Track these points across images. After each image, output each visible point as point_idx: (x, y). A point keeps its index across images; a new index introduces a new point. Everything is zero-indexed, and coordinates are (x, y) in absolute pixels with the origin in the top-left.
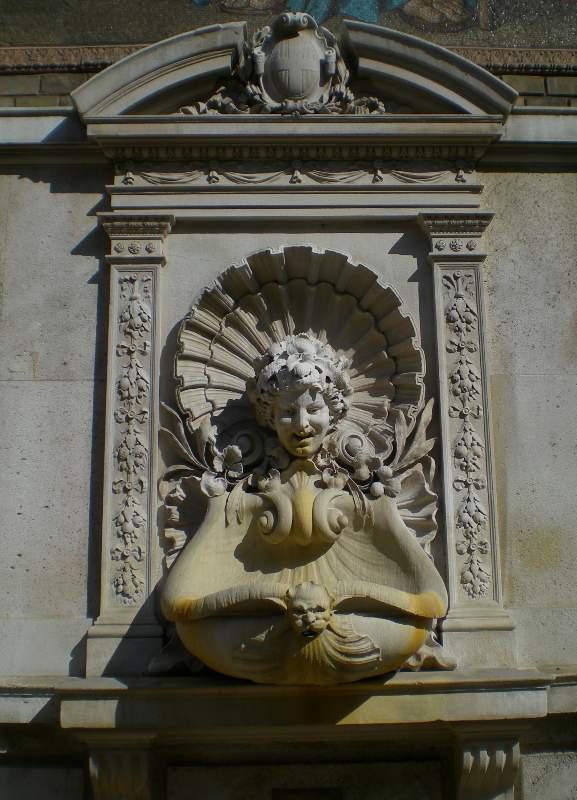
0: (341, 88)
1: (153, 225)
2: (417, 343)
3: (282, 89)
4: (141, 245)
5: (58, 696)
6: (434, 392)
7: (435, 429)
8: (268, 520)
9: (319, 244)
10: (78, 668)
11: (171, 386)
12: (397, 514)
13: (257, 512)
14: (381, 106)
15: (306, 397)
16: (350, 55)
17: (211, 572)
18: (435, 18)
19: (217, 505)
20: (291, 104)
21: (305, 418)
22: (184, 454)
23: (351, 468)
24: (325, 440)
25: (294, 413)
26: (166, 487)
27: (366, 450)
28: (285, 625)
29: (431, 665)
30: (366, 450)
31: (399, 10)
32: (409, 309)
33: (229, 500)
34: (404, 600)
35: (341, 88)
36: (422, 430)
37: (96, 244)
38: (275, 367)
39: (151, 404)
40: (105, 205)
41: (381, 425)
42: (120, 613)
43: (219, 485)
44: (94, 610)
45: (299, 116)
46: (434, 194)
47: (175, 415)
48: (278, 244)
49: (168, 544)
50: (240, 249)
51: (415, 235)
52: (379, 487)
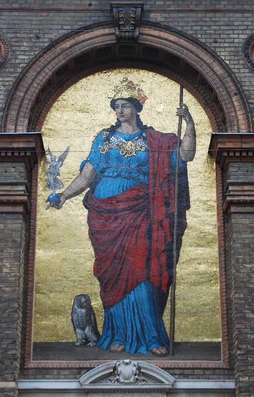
18: (160, 353)
31: (151, 351)
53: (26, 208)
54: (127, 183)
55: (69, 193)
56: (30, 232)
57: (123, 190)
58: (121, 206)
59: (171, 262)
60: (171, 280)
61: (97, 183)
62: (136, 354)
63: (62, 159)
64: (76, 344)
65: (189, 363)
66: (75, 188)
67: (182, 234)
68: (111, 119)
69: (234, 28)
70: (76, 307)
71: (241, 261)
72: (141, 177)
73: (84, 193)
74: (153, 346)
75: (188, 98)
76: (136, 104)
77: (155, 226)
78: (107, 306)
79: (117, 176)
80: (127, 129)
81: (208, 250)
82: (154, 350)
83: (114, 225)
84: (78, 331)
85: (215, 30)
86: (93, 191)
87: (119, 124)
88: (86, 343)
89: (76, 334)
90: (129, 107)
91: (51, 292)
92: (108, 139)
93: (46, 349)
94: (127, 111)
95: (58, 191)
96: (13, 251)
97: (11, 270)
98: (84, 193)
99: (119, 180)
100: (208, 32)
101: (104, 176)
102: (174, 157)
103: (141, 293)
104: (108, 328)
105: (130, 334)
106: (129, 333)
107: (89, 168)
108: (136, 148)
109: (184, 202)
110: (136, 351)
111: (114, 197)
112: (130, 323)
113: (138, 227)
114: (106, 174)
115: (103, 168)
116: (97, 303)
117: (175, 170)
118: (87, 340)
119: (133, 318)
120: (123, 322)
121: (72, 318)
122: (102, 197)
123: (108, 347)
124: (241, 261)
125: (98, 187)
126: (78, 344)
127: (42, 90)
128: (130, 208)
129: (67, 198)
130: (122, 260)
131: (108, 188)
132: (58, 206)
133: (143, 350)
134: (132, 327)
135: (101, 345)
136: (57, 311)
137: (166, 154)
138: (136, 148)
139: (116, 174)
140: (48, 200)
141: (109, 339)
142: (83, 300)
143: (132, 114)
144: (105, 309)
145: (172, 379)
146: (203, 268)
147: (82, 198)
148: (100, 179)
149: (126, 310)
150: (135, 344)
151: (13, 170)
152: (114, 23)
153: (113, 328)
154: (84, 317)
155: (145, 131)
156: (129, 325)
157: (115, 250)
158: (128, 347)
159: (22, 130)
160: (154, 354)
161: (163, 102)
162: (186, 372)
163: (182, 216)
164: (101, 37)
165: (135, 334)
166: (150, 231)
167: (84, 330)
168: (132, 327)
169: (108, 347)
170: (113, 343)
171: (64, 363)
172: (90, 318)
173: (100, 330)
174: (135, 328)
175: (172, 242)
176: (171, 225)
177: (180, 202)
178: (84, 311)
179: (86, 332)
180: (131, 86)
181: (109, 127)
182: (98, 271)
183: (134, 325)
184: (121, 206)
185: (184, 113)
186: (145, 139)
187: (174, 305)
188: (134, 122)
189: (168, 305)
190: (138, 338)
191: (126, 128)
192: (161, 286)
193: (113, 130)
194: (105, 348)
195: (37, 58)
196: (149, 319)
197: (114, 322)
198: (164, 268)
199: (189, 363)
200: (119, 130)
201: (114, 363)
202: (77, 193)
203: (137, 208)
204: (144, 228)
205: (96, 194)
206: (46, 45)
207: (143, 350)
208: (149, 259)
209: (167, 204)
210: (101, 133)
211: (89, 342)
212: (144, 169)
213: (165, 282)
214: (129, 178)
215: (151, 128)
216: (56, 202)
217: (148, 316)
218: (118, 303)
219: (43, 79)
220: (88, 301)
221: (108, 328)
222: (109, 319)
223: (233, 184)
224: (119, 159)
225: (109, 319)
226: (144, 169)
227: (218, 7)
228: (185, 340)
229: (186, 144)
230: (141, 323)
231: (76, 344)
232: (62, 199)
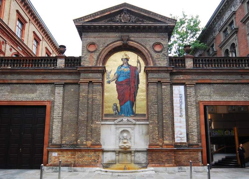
9: (126, 129)
48: (124, 129)
50: (122, 129)
53: (102, 84)
54: (125, 78)
55: (112, 80)
58: (124, 83)
59: (135, 96)
60: (135, 100)
62: (127, 116)
63: (110, 72)
65: (139, 118)
66: (113, 79)
67: (138, 90)
68: (121, 63)
72: (128, 77)
73: (115, 80)
75: (140, 58)
76: (127, 59)
77: (131, 88)
78: (121, 106)
80: (125, 65)
81: (143, 93)
82: (131, 115)
83: (122, 87)
86: (117, 80)
87: (123, 64)
91: (108, 103)
92: (121, 67)
93: (107, 115)
94: (125, 61)
95: (109, 80)
98: (115, 80)
107: (116, 74)
108: (127, 70)
109: (138, 83)
111: (122, 81)
113: (128, 88)
116: (118, 105)
118: (116, 113)
125: (118, 79)
127: (105, 56)
128: (126, 84)
129: (112, 81)
131: (121, 79)
133: (129, 115)
136: (109, 107)
137: (134, 71)
138: (127, 70)
140: (107, 82)
143: (126, 62)
145: (135, 122)
146: (142, 97)
147: (115, 81)
150: (127, 114)
152: (122, 40)
155: (129, 66)
157: (122, 93)
159: (101, 65)
160: (131, 116)
161: (134, 59)
162: (138, 120)
163: (138, 85)
164: (119, 43)
166: (130, 89)
171: (111, 118)
176: (135, 87)
177: (137, 82)
178: (115, 107)
180: (126, 55)
182: (119, 98)
184: (124, 83)
185: (138, 62)
186: (129, 68)
188: (127, 64)
189: (134, 105)
190: (128, 113)
191: (125, 65)
193: (122, 66)
195: (104, 49)
198: (134, 98)
199: (139, 118)
200: (123, 66)
201: (122, 118)
202: (113, 80)
204: (129, 88)
205: (118, 81)
207: (129, 115)
208: (130, 96)
209: (134, 83)
210: (119, 66)
213: (134, 101)
216: (109, 82)
217: (130, 108)
219: (105, 53)
220: (116, 105)
223: (149, 78)
224: (123, 72)
227: (146, 36)
228: (138, 113)
229: (139, 69)
232: (110, 82)
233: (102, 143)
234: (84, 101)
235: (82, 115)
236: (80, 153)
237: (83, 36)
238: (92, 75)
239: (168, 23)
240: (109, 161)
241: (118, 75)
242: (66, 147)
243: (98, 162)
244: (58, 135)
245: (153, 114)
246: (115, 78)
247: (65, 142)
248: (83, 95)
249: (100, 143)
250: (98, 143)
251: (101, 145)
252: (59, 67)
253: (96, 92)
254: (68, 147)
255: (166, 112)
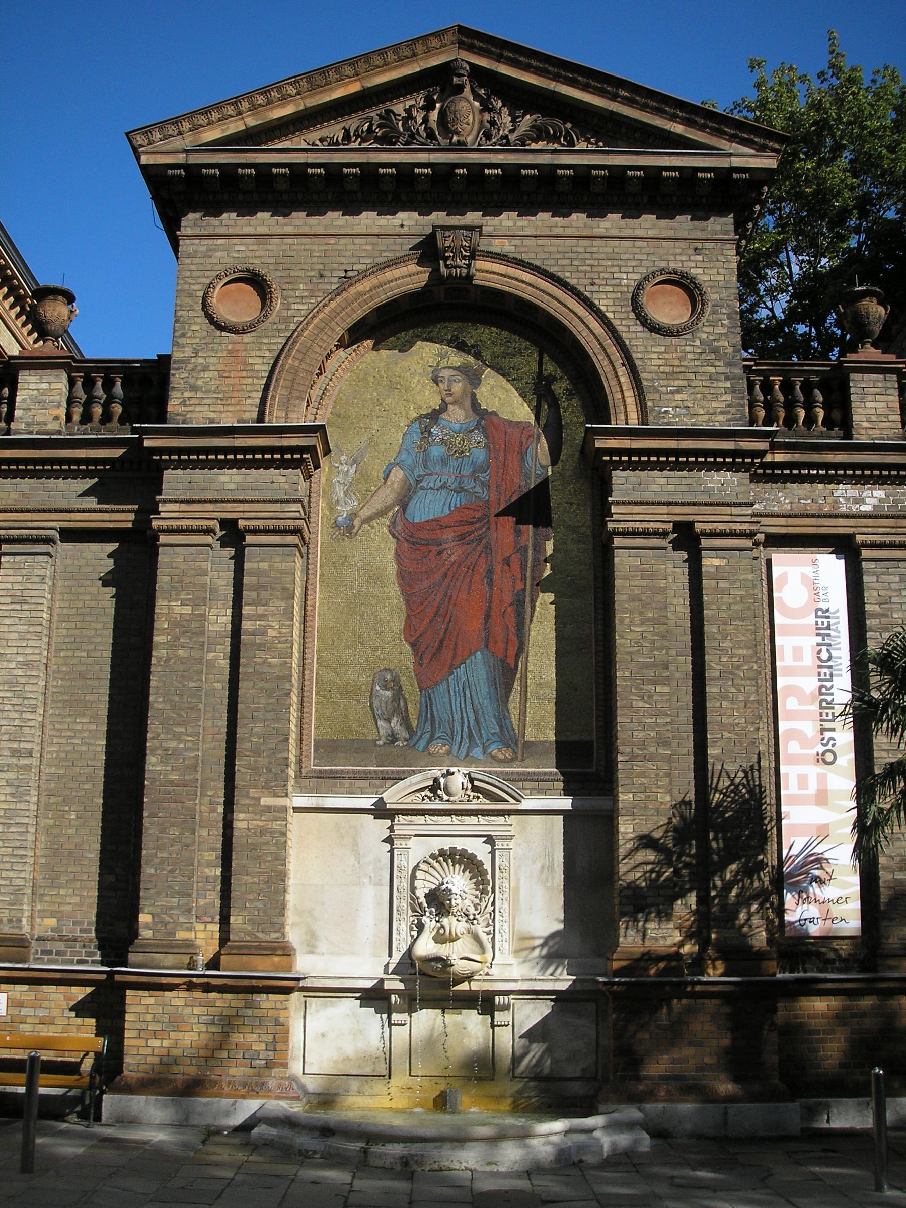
0: (468, 792)
1: (407, 837)
2: (489, 877)
3: (448, 794)
4: (403, 843)
5: (382, 981)
6: (493, 892)
7: (493, 904)
8: (442, 931)
9: (460, 844)
10: (386, 972)
11: (413, 889)
12: (480, 929)
13: (439, 929)
14: (481, 796)
15: (454, 896)
16: (471, 780)
17: (426, 947)
19: (427, 926)
20: (452, 799)
21: (453, 902)
22: (417, 909)
23: (467, 915)
24: (459, 907)
25: (450, 900)
26: (412, 919)
27: (472, 910)
28: (445, 963)
29: (487, 974)
30: (472, 910)
32: (487, 866)
33: (430, 923)
34: (478, 958)
35: (468, 792)
36: (490, 904)
37: (389, 840)
38: (444, 887)
39: (406, 894)
40: (391, 829)
41: (477, 901)
42: (397, 957)
43: (428, 920)
44: (390, 955)
45: (454, 802)
46: (496, 826)
47: (414, 898)
48: (447, 844)
49: (412, 936)
51: (490, 840)
52: (475, 922)
54: (457, 500)
56: (307, 574)
57: (450, 509)
61: (410, 499)
62: (468, 759)
64: (378, 743)
69: (620, 263)
70: (378, 688)
71: (627, 621)
72: (478, 489)
74: (493, 747)
75: (550, 368)
77: (498, 568)
79: (441, 487)
84: (381, 723)
85: (592, 266)
86: (404, 507)
87: (444, 407)
88: (393, 742)
89: (378, 729)
90: (459, 381)
92: (427, 431)
94: (457, 387)
96: (283, 604)
97: (280, 633)
98: (390, 514)
99: (444, 492)
100: (581, 268)
101: (422, 488)
102: (529, 459)
103: (476, 670)
104: (426, 721)
105: (459, 729)
106: (457, 727)
107: (397, 475)
110: (467, 755)
111: (436, 520)
112: (459, 713)
114: (423, 484)
115: (419, 476)
117: (530, 478)
118: (393, 738)
119: (463, 706)
120: (449, 712)
121: (371, 704)
122: (417, 520)
123: (426, 747)
124: (627, 621)
126: (381, 743)
130: (448, 616)
131: (429, 507)
132: (351, 533)
133: (477, 752)
134: (462, 718)
135: (414, 746)
139: (439, 484)
141: (428, 736)
142: (389, 677)
143: (464, 391)
144: (421, 691)
148: (415, 492)
149: (452, 693)
151: (283, 479)
153: (433, 721)
154: (389, 703)
156: (457, 717)
158: (455, 748)
160: (494, 758)
165: (466, 729)
167: (390, 722)
168: (462, 718)
169: (426, 747)
170: (435, 742)
172: (399, 704)
173: (414, 724)
174: (466, 720)
175: (524, 590)
178: (389, 693)
179: (392, 725)
181: (430, 411)
183: (465, 715)
187: (526, 687)
188: (468, 403)
189: (517, 685)
192: (506, 657)
193: (435, 416)
194: (421, 749)
195: (318, 308)
196: (488, 708)
197: (434, 709)
201: (437, 772)
203: (472, 537)
204: (482, 569)
206: (334, 287)
207: (477, 752)
211: (397, 740)
212: (483, 477)
213: (512, 652)
214: (460, 490)
215: (495, 413)
218: (442, 680)
221: (426, 721)
222: (426, 706)
223: (617, 503)
225: (426, 706)
226: (483, 477)
230: (475, 712)
231: (378, 743)
233: (294, 936)
234: (181, 653)
235: (166, 750)
236: (151, 1000)
237: (189, 231)
238: (239, 478)
239: (731, 155)
240: (347, 1059)
241: (405, 480)
242: (58, 953)
243: (269, 1065)
244: (11, 874)
245: (643, 745)
246: (389, 501)
247: (52, 922)
248: (178, 610)
249: (283, 935)
250: (274, 936)
251: (286, 951)
252: (28, 424)
253: (264, 595)
254: (73, 954)
255: (726, 735)
